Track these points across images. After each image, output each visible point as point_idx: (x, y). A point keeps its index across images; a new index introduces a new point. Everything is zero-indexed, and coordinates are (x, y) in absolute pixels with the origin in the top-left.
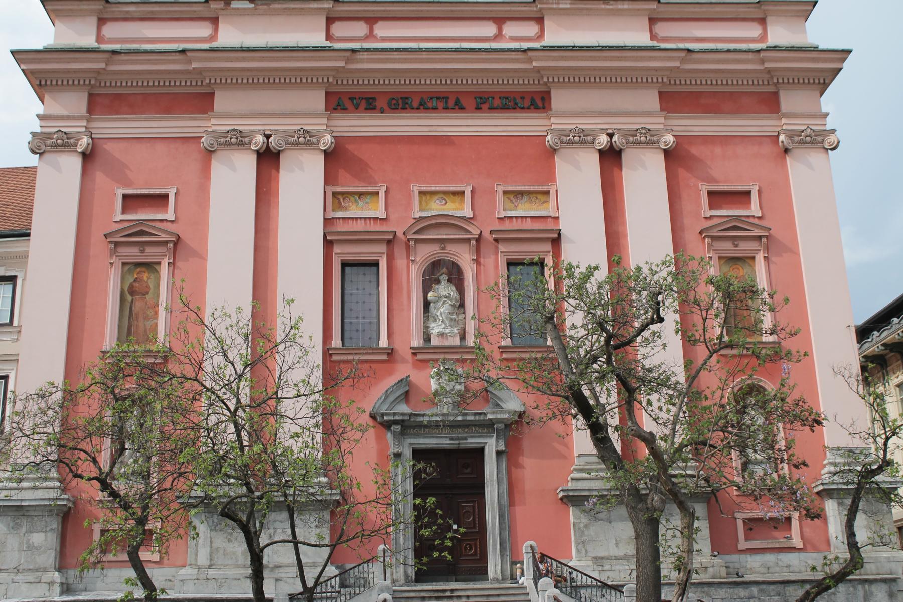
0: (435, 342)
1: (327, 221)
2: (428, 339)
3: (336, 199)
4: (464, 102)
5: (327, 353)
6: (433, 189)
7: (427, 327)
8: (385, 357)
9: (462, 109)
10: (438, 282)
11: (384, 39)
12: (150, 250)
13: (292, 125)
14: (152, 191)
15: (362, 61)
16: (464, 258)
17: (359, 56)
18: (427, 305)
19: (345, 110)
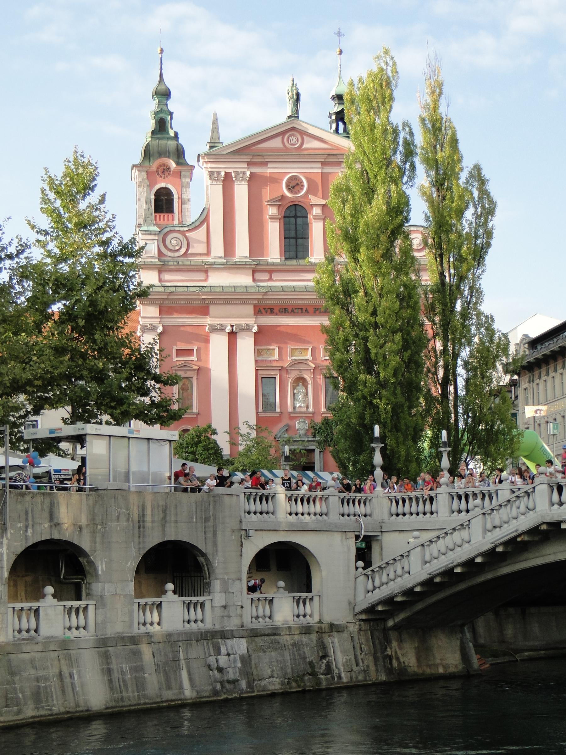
0: (297, 410)
1: (256, 361)
2: (294, 408)
3: (258, 352)
4: (309, 310)
5: (257, 413)
6: (296, 348)
7: (294, 404)
8: (279, 415)
9: (308, 313)
10: (298, 385)
11: (275, 281)
12: (188, 373)
13: (243, 322)
14: (187, 348)
15: (269, 295)
16: (308, 377)
17: (268, 293)
18: (294, 394)
19: (261, 313)
